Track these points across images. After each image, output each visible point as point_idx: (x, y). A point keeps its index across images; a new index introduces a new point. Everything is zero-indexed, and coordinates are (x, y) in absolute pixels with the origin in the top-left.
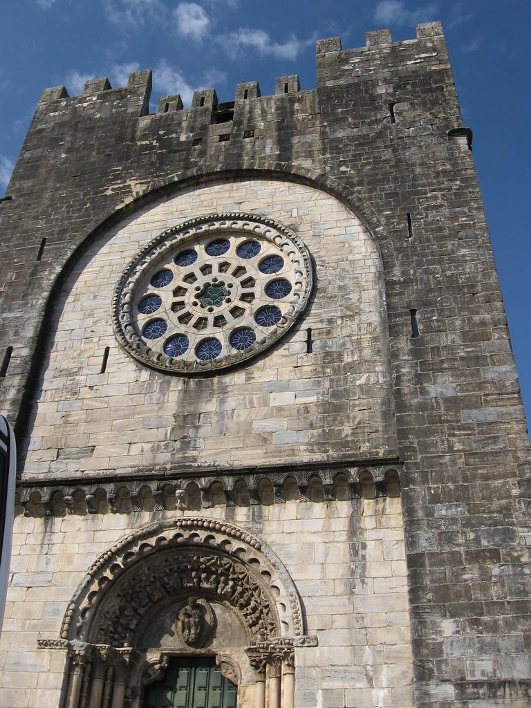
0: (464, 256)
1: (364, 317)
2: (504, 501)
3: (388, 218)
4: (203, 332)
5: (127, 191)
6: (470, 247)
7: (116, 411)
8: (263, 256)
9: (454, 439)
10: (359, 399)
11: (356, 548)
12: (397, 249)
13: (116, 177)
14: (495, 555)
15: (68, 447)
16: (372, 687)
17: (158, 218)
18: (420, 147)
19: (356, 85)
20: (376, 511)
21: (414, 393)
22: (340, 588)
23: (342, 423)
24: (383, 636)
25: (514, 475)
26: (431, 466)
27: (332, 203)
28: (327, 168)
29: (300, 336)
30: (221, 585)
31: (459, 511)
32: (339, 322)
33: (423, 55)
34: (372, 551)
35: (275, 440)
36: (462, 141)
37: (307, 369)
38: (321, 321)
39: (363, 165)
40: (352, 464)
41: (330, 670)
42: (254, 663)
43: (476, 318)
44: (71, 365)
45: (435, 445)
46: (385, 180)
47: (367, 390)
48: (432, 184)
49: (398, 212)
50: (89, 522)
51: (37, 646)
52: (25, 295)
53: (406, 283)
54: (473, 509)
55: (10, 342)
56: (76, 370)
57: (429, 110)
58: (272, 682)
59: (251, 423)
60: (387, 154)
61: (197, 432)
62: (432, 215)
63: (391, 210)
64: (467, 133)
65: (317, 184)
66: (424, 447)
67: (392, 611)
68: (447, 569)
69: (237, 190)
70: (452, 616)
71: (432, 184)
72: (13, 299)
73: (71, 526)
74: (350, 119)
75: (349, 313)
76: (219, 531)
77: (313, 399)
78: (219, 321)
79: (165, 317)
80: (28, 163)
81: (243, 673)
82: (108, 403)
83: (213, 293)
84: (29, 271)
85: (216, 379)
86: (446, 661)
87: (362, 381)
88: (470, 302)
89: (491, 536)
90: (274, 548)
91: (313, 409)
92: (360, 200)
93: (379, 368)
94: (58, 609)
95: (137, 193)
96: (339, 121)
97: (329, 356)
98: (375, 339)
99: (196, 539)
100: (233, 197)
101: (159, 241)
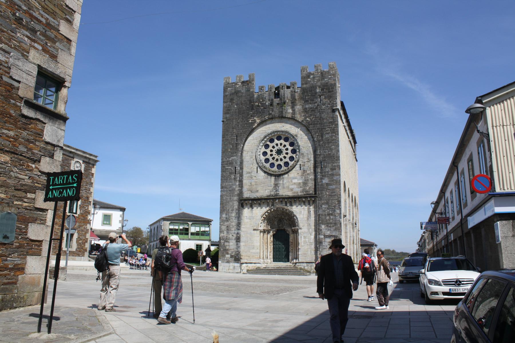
5: (255, 121)
13: (252, 116)
14: (332, 214)
17: (264, 129)
21: (320, 182)
22: (306, 219)
29: (298, 167)
35: (294, 190)
46: (317, 124)
47: (311, 179)
53: (320, 155)
54: (329, 206)
57: (329, 99)
62: (327, 136)
66: (321, 193)
78: (281, 160)
83: (279, 152)
89: (331, 211)
96: (306, 101)
97: (304, 171)
101: (265, 137)
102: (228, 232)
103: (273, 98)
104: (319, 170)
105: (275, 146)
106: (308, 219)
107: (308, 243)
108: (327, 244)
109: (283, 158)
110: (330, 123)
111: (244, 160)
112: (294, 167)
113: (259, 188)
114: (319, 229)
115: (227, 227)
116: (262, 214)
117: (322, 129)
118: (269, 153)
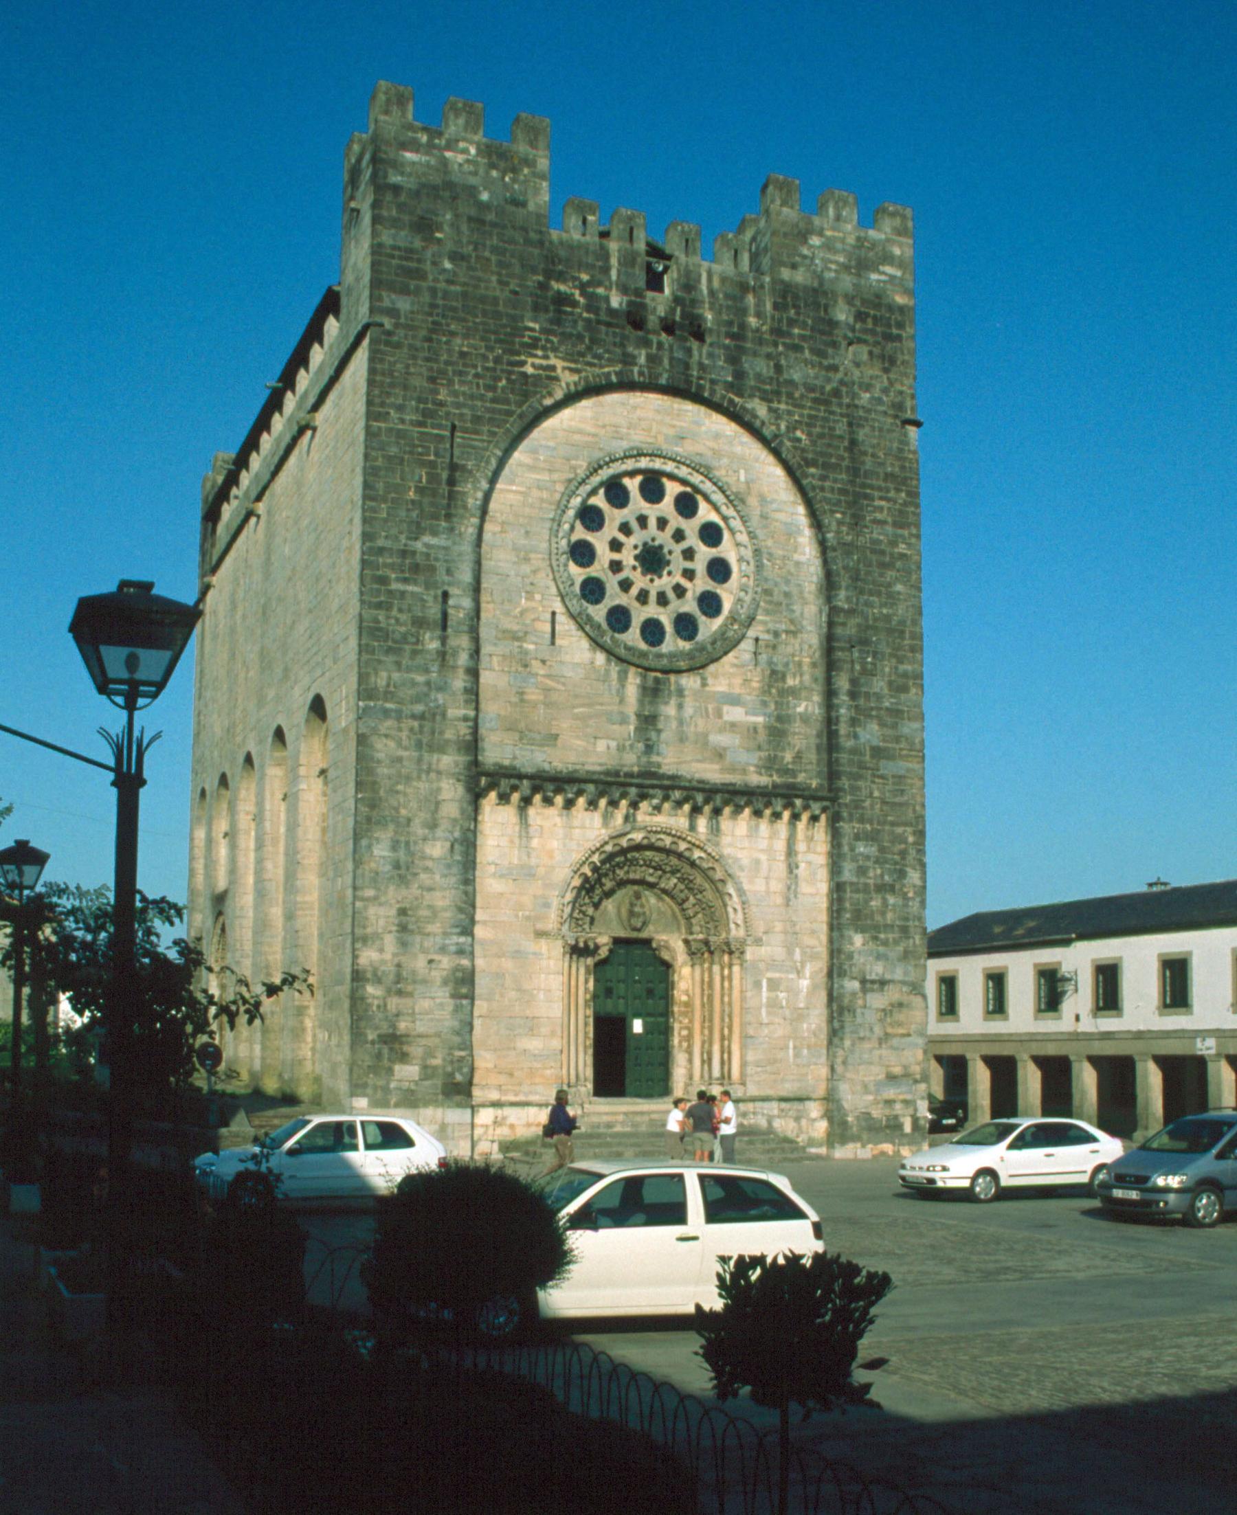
0: (899, 593)
1: (805, 636)
2: (903, 846)
3: (840, 523)
4: (645, 608)
6: (904, 584)
7: (576, 696)
8: (703, 521)
9: (874, 786)
10: (797, 727)
11: (792, 868)
12: (844, 568)
13: (534, 344)
14: (892, 889)
15: (530, 731)
16: (799, 977)
18: (873, 428)
19: (815, 291)
20: (807, 837)
22: (779, 900)
23: (783, 750)
24: (809, 941)
25: (911, 825)
26: (857, 807)
27: (779, 472)
28: (783, 427)
29: (747, 646)
31: (873, 850)
32: (784, 636)
33: (888, 269)
34: (802, 870)
35: (729, 757)
36: (912, 431)
37: (755, 685)
38: (768, 632)
39: (821, 436)
40: (797, 796)
41: (772, 964)
43: (902, 668)
44: (515, 628)
45: (859, 789)
46: (836, 467)
47: (805, 719)
48: (880, 489)
49: (848, 520)
52: (448, 517)
53: (851, 612)
54: (882, 850)
55: (443, 583)
56: (521, 634)
57: (886, 371)
58: (716, 968)
59: (706, 735)
60: (841, 428)
61: (659, 735)
63: (843, 513)
64: (918, 424)
65: (772, 445)
66: (855, 789)
67: (815, 921)
68: (860, 896)
69: (678, 415)
70: (862, 932)
71: (880, 489)
72: (435, 517)
73: (546, 817)
74: (807, 352)
75: (792, 628)
76: (684, 839)
77: (760, 719)
79: (603, 578)
80: (393, 257)
82: (564, 684)
83: (652, 560)
84: (445, 475)
85: (672, 677)
86: (855, 965)
87: (800, 709)
88: (898, 649)
89: (891, 872)
91: (761, 730)
92: (814, 488)
93: (817, 698)
95: (568, 385)
98: (814, 665)
100: (674, 426)
102: (403, 944)
103: (642, 283)
104: (842, 683)
105: (634, 525)
106: (788, 900)
107: (787, 1012)
108: (871, 1017)
109: (671, 595)
110: (888, 477)
111: (486, 564)
112: (725, 644)
113: (564, 725)
114: (839, 951)
115: (403, 912)
116: (577, 856)
117: (857, 496)
118: (604, 555)
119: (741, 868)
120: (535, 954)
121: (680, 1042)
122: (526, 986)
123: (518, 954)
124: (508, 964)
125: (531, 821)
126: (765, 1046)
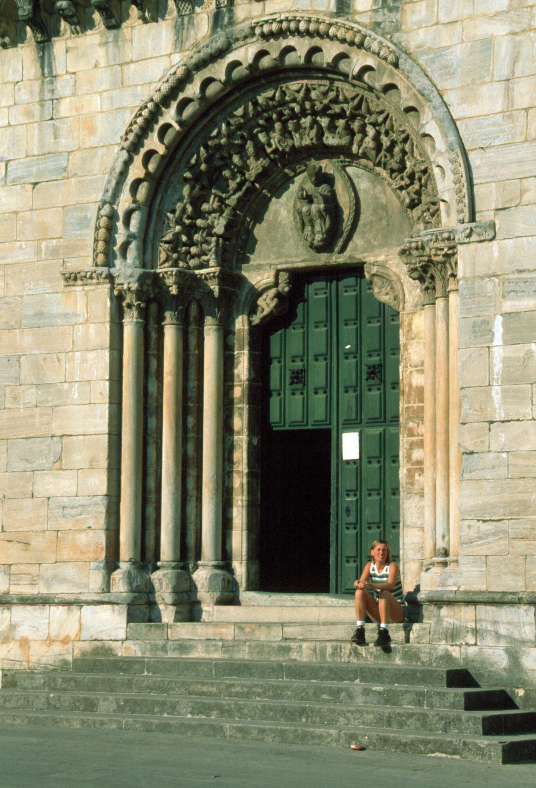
30: (358, 137)
42: (415, 275)
50: (111, 46)
51: (63, 283)
81: (406, 292)
90: (422, 61)
94: (86, 217)
99: (290, 59)
119: (448, 71)
120: (65, 315)
121: (410, 474)
122: (51, 378)
123: (41, 320)
124: (26, 340)
125: (59, 68)
126: (503, 472)
